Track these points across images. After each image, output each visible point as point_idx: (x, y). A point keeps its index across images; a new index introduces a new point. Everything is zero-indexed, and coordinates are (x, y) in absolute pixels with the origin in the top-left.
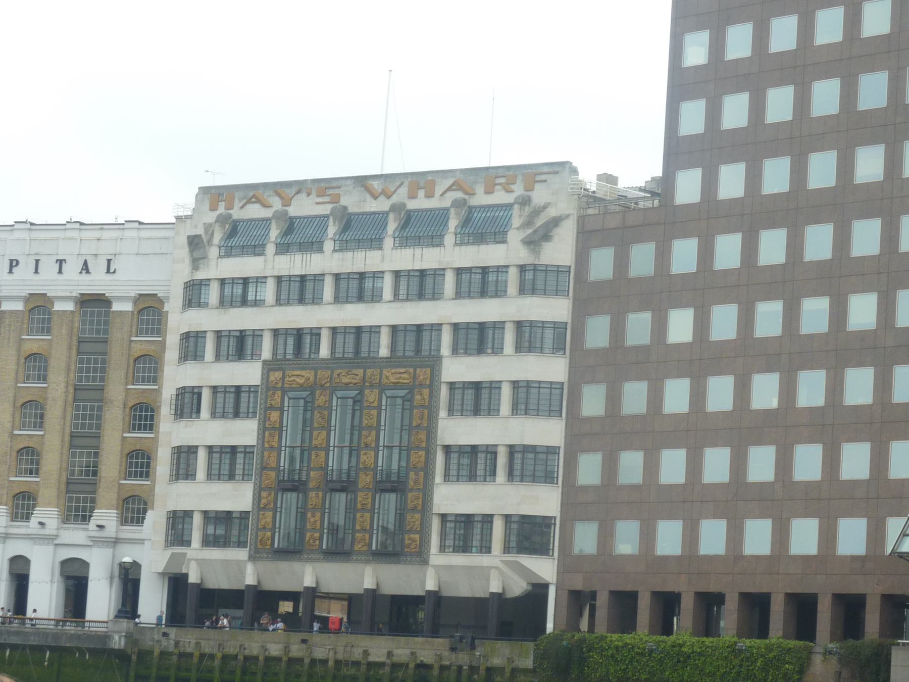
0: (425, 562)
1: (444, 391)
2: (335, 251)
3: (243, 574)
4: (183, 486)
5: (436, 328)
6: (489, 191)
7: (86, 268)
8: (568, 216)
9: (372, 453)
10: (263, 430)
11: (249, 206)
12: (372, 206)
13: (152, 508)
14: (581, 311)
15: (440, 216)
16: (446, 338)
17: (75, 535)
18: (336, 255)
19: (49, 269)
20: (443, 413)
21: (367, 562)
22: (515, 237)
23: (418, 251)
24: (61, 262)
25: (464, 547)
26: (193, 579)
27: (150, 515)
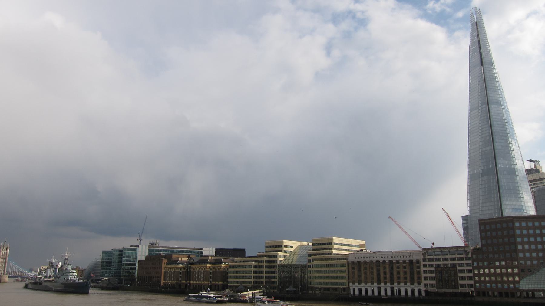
0: (458, 289)
1: (458, 271)
3: (435, 290)
5: (456, 264)
6: (460, 249)
7: (409, 257)
10: (436, 275)
13: (422, 283)
16: (457, 265)
17: (413, 287)
19: (405, 257)
22: (464, 254)
24: (406, 256)
26: (429, 291)
27: (421, 284)
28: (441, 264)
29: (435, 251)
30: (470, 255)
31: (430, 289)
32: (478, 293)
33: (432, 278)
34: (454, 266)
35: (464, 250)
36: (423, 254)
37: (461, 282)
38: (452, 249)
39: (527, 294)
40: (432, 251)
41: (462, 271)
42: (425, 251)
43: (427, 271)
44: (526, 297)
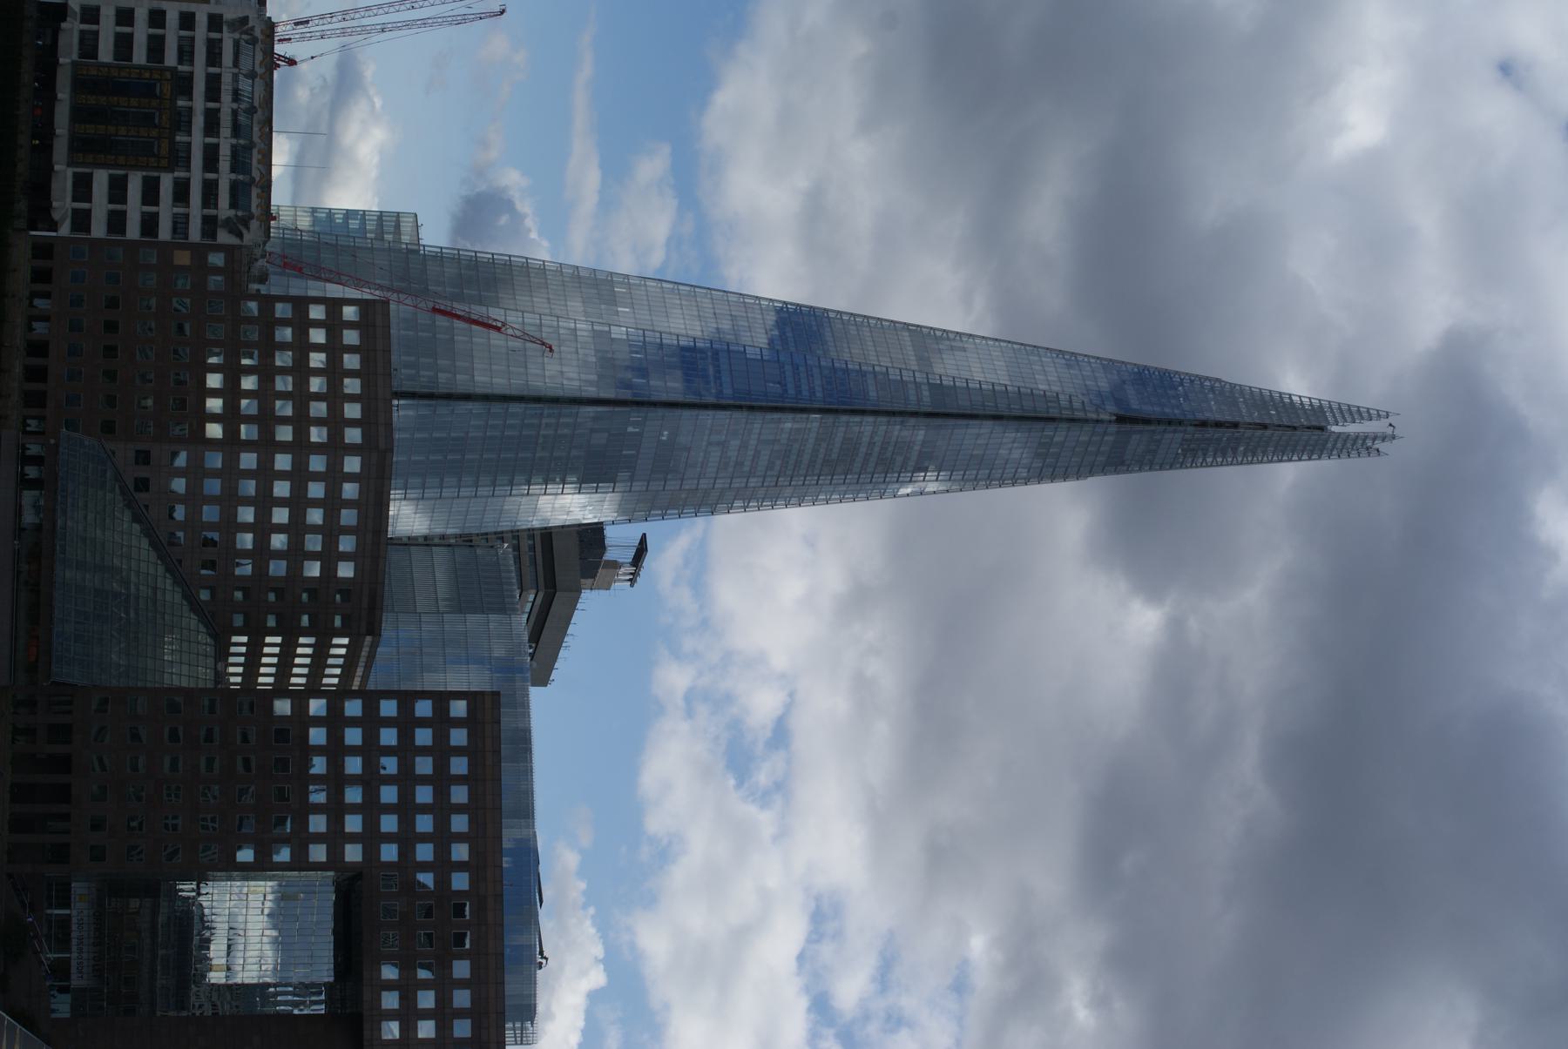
0: (69, 165)
1: (156, 174)
2: (232, 109)
4: (112, 19)
5: (188, 168)
6: (258, 196)
8: (243, 241)
9: (125, 134)
10: (140, 67)
11: (261, 53)
12: (256, 129)
14: (193, 247)
15: (247, 171)
16: (181, 174)
18: (230, 110)
20: (144, 173)
21: (69, 130)
22: (232, 213)
23: (229, 158)
25: (75, 185)
26: (63, 25)
28: (191, 100)
29: (257, 80)
30: (224, 237)
31: (72, 29)
32: (43, 250)
33: (124, 45)
34: (180, 158)
35: (251, 217)
36: (245, 20)
37: (101, 179)
38: (259, 162)
39: (37, 460)
40: (257, 62)
41: (151, 193)
42: (258, 33)
43: (163, 26)
44: (23, 452)
